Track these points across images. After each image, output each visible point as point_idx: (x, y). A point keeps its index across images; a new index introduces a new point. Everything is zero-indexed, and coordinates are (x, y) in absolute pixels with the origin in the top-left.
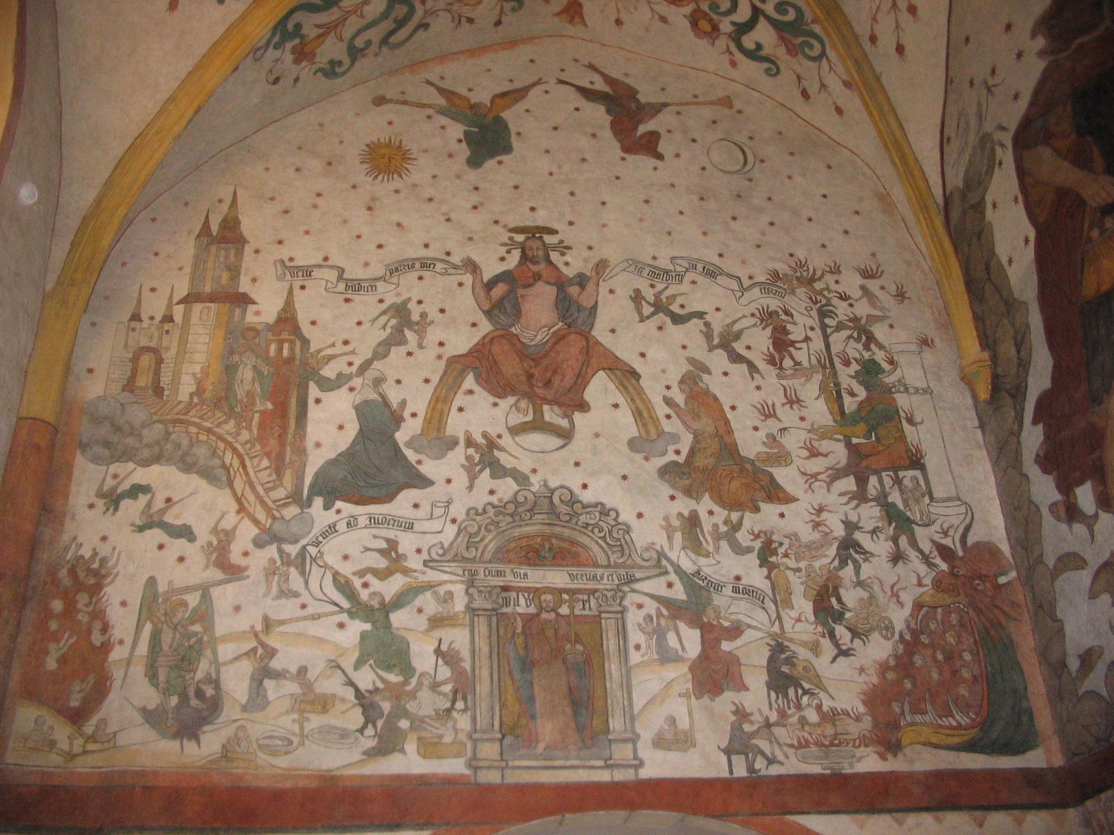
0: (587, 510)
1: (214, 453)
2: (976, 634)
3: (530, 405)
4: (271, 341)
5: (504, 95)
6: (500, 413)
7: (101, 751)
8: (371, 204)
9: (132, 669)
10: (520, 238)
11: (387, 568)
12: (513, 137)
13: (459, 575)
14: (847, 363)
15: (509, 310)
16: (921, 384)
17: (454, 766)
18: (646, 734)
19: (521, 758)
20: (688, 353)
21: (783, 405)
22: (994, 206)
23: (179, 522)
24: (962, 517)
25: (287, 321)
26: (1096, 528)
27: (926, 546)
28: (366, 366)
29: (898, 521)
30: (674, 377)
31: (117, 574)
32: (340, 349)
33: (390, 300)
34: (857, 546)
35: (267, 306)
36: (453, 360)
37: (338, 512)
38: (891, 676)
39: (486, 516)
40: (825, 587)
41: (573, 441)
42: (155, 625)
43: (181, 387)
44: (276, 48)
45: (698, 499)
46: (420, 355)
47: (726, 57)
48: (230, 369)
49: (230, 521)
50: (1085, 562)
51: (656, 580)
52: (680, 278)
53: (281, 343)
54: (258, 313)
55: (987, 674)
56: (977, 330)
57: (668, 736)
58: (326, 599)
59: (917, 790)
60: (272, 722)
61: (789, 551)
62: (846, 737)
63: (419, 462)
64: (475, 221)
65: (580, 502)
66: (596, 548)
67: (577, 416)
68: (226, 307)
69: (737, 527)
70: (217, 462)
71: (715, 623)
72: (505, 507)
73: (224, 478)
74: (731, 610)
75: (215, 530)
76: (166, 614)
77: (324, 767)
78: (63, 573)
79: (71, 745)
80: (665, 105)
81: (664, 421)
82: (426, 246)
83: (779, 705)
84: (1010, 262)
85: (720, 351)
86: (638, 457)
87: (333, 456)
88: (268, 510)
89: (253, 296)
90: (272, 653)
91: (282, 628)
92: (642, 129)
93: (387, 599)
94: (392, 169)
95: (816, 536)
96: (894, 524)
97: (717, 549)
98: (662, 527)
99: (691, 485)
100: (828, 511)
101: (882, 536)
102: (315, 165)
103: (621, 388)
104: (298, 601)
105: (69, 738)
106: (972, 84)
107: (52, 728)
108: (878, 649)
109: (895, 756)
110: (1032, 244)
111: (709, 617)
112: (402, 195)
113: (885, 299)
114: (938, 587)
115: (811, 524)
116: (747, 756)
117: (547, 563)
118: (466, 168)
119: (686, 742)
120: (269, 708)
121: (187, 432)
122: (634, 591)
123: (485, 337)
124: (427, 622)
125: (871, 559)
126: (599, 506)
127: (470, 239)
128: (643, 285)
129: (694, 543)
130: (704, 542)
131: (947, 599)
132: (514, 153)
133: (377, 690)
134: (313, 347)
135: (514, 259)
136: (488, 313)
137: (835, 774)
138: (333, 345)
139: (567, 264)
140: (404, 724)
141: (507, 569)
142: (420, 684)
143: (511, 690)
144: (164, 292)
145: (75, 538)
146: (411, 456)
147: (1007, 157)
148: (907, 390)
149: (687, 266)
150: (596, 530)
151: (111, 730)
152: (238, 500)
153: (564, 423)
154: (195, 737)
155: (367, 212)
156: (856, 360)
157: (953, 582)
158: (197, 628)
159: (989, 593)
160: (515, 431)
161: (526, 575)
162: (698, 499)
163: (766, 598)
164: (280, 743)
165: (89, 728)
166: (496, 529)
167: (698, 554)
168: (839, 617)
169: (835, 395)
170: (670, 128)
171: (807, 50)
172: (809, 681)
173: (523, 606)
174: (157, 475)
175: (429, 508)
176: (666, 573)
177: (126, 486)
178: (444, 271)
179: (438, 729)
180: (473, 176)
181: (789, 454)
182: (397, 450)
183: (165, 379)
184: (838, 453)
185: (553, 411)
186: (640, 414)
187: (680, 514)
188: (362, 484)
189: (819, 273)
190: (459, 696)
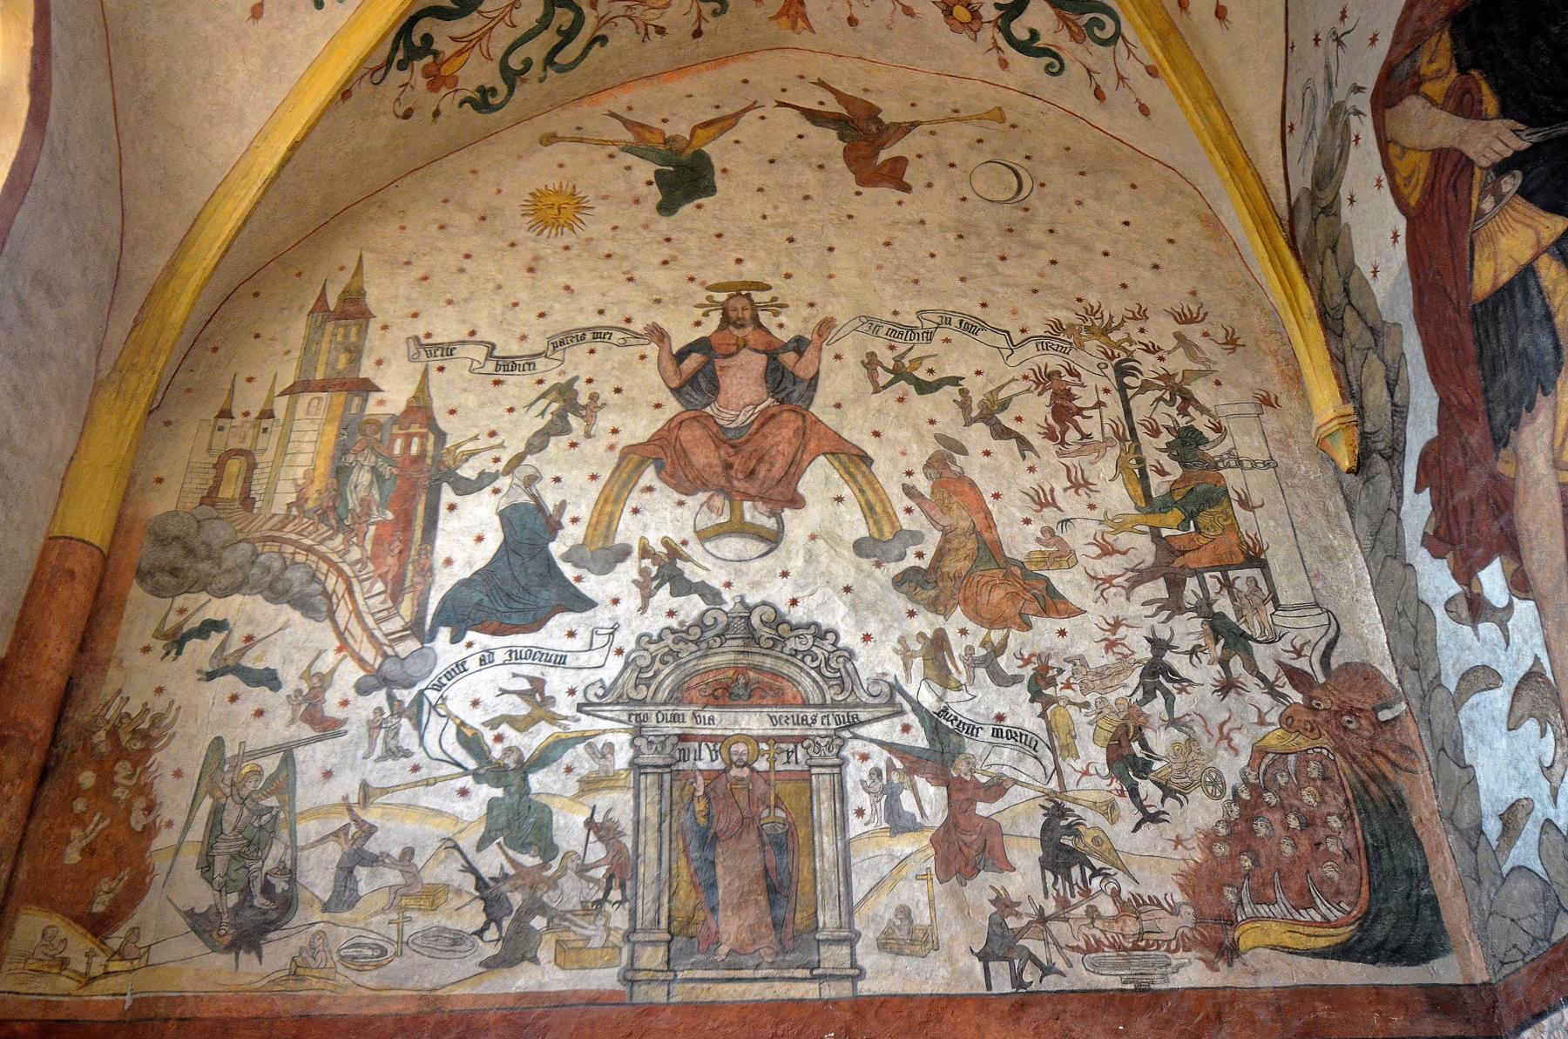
0: (795, 633)
2: (1348, 791)
3: (727, 502)
4: (398, 436)
6: (686, 514)
7: (128, 971)
8: (533, 265)
9: (180, 859)
10: (721, 297)
11: (529, 715)
12: (718, 173)
13: (621, 722)
14: (1155, 433)
15: (703, 386)
17: (605, 979)
18: (869, 935)
19: (694, 967)
20: (935, 429)
21: (1065, 490)
22: (1352, 201)
23: (261, 666)
24: (1323, 630)
25: (420, 410)
26: (1510, 624)
28: (518, 459)
30: (917, 460)
31: (174, 735)
32: (484, 442)
33: (552, 379)
34: (1170, 673)
37: (470, 645)
38: (1221, 850)
39: (662, 644)
41: (781, 545)
42: (216, 800)
43: (277, 496)
44: (402, 66)
45: (946, 616)
46: (586, 446)
47: (994, 54)
48: (340, 472)
50: (1500, 678)
51: (887, 722)
53: (408, 439)
54: (381, 403)
55: (1366, 847)
56: (1337, 377)
57: (901, 934)
58: (445, 758)
60: (362, 925)
61: (1072, 681)
62: (1155, 936)
63: (578, 579)
64: (663, 280)
65: (788, 623)
66: (807, 682)
67: (787, 513)
68: (340, 397)
70: (316, 587)
71: (968, 778)
72: (687, 632)
73: (324, 608)
74: (989, 761)
75: (306, 675)
76: (233, 784)
77: (427, 986)
79: (89, 964)
80: (914, 124)
82: (601, 312)
83: (1058, 894)
84: (1375, 272)
85: (981, 425)
86: (867, 564)
87: (467, 575)
89: (377, 382)
90: (369, 831)
91: (384, 799)
93: (527, 756)
94: (562, 221)
95: (1110, 659)
96: (1222, 642)
97: (972, 678)
98: (896, 651)
99: (937, 597)
100: (1127, 626)
101: (1204, 658)
102: (466, 221)
103: (846, 476)
104: (407, 763)
105: (86, 955)
106: (1317, 40)
107: (64, 941)
109: (1230, 965)
110: (1402, 240)
111: (959, 770)
112: (574, 252)
114: (1290, 726)
115: (1103, 643)
116: (1011, 961)
117: (741, 702)
118: (656, 215)
119: (926, 942)
120: (358, 905)
121: (280, 553)
122: (856, 737)
123: (672, 419)
124: (577, 784)
125: (1189, 689)
126: (813, 627)
127: (658, 301)
128: (879, 346)
129: (940, 672)
130: (953, 670)
131: (1303, 742)
132: (718, 194)
133: (506, 876)
136: (676, 391)
137: (1141, 991)
138: (476, 438)
139: (781, 326)
140: (539, 922)
142: (563, 869)
143: (684, 872)
145: (120, 691)
146: (569, 571)
147: (1364, 127)
148: (1240, 464)
149: (939, 320)
150: (808, 659)
151: (143, 942)
152: (340, 635)
153: (770, 523)
155: (527, 274)
156: (1167, 428)
157: (1310, 719)
158: (272, 801)
159: (1367, 734)
160: (703, 536)
161: (712, 719)
162: (946, 616)
163: (1040, 743)
164: (369, 953)
165: (114, 943)
166: (675, 660)
167: (946, 687)
168: (1143, 769)
170: (920, 152)
171: (1097, 31)
172: (1101, 857)
173: (706, 761)
175: (587, 635)
176: (901, 712)
177: (195, 622)
178: (622, 341)
179: (583, 927)
180: (664, 224)
181: (1072, 552)
183: (258, 487)
184: (1142, 548)
185: (755, 508)
186: (871, 507)
187: (921, 635)
188: (502, 609)
189: (1116, 321)
190: (615, 882)
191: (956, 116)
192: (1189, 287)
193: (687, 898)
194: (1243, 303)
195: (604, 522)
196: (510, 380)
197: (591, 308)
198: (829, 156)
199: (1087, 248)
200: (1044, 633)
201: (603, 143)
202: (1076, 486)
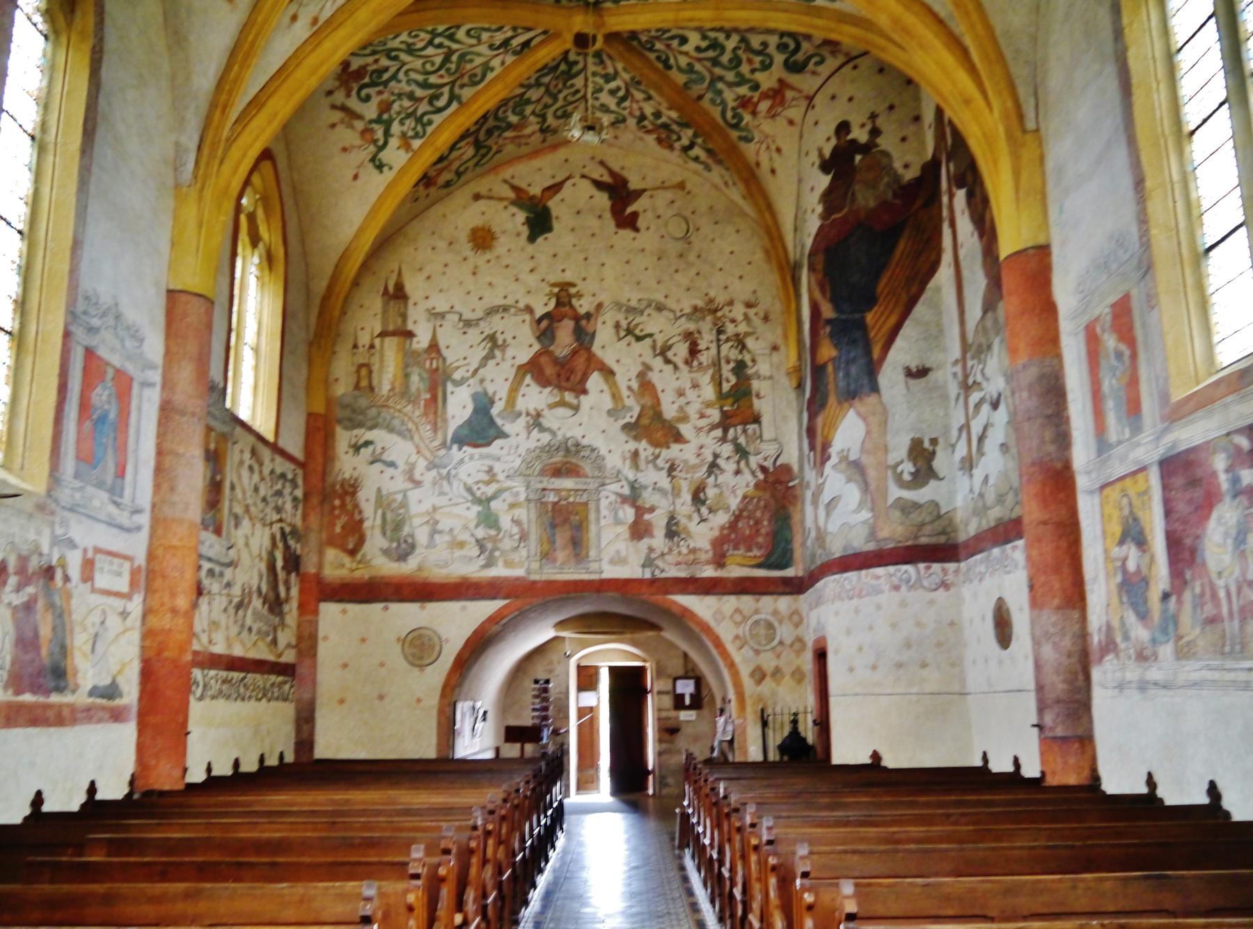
1: (403, 423)
4: (425, 360)
5: (549, 188)
16: (768, 374)
17: (519, 572)
18: (606, 557)
25: (434, 347)
28: (476, 371)
29: (742, 453)
32: (462, 362)
35: (422, 340)
36: (520, 367)
48: (407, 376)
49: (414, 458)
52: (642, 312)
53: (432, 359)
54: (418, 342)
59: (729, 585)
64: (532, 280)
67: (582, 397)
68: (401, 339)
69: (657, 457)
70: (404, 428)
75: (407, 463)
78: (338, 487)
80: (644, 191)
86: (612, 420)
88: (431, 452)
90: (437, 522)
92: (629, 210)
97: (647, 468)
102: (442, 245)
108: (722, 518)
111: (639, 503)
113: (757, 321)
128: (621, 317)
131: (760, 494)
134: (448, 362)
136: (538, 338)
141: (545, 479)
142: (504, 536)
144: (368, 331)
146: (499, 421)
151: (368, 558)
152: (417, 447)
153: (575, 402)
160: (552, 406)
165: (359, 557)
168: (703, 502)
169: (718, 381)
173: (552, 498)
176: (620, 481)
177: (361, 441)
180: (530, 248)
184: (715, 415)
191: (663, 187)
192: (752, 289)
193: (546, 547)
195: (511, 401)
197: (502, 295)
200: (674, 451)
201: (501, 199)
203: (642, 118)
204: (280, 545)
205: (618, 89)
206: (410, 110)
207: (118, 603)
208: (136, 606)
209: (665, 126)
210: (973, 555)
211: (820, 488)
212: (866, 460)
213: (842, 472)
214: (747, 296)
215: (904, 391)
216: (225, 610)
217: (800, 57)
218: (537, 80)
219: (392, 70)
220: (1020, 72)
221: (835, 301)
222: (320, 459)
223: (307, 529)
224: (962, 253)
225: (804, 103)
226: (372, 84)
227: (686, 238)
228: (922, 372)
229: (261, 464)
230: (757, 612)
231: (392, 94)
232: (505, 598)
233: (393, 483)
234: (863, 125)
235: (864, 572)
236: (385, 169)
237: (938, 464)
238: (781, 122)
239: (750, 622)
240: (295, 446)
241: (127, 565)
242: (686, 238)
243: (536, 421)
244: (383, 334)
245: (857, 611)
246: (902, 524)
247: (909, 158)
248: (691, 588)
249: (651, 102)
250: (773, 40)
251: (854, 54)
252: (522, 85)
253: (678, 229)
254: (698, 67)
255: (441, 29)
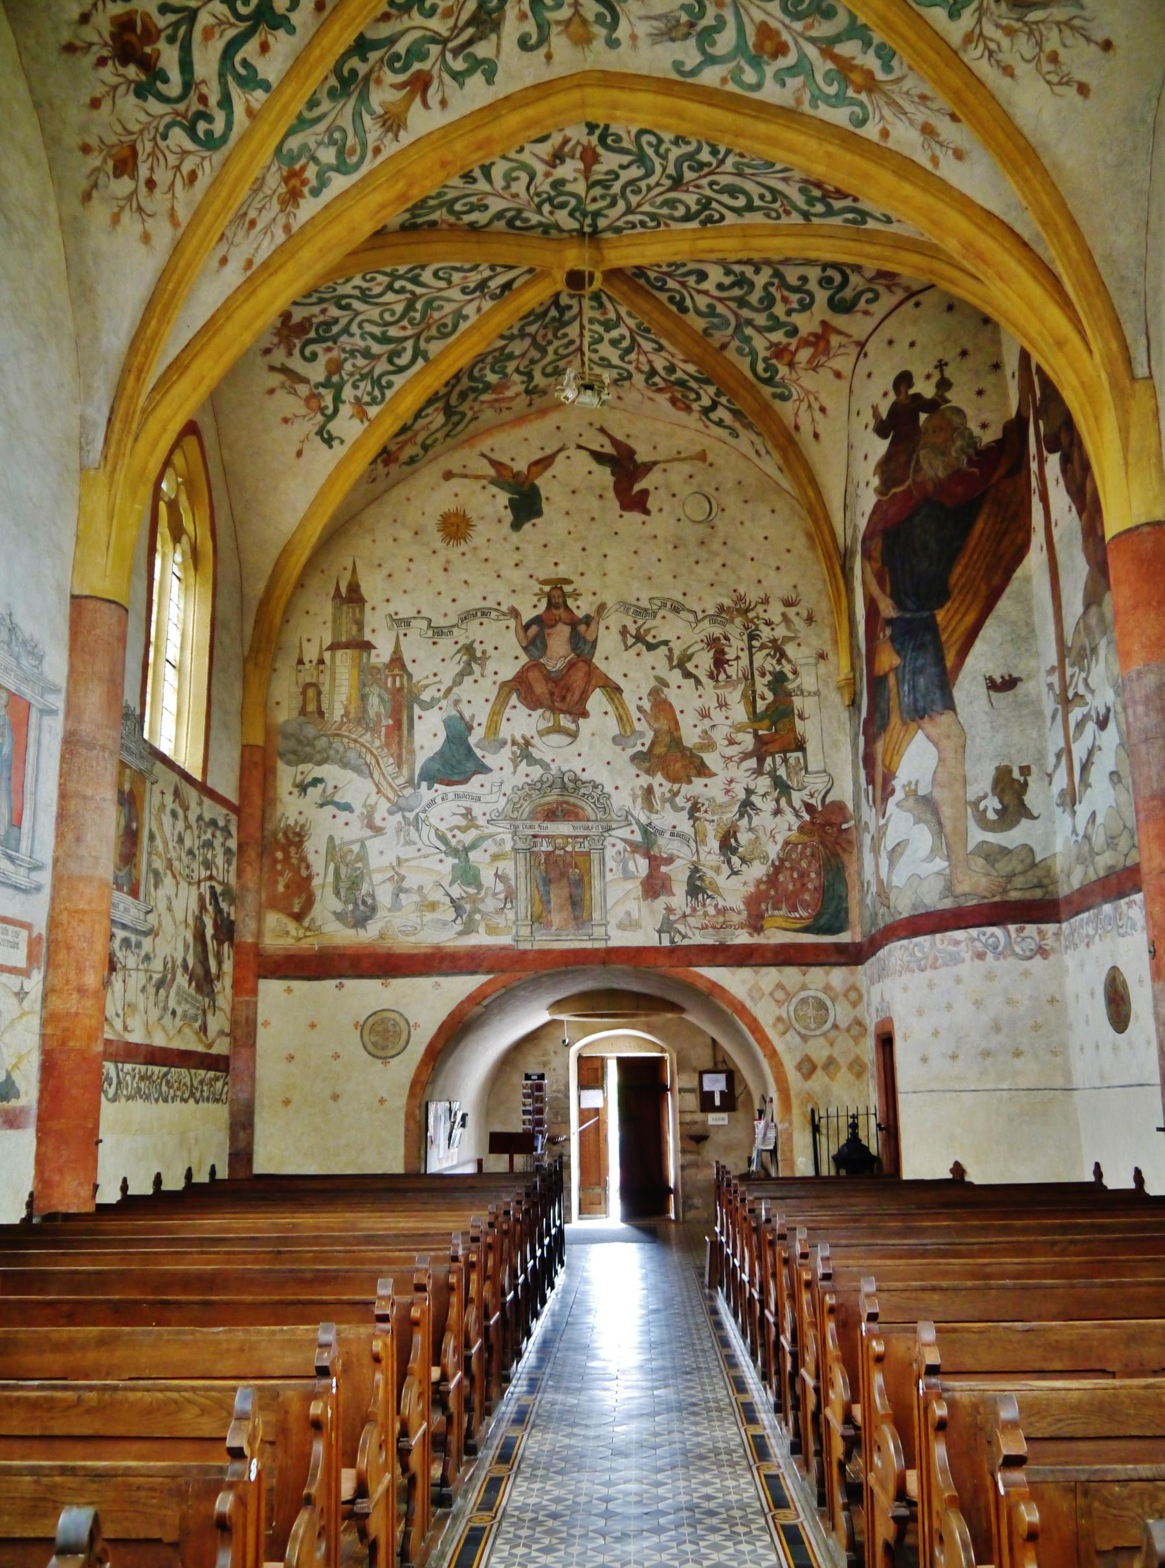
5: (537, 463)
6: (532, 720)
10: (547, 588)
14: (763, 675)
16: (813, 689)
17: (505, 940)
20: (656, 672)
23: (343, 801)
25: (397, 661)
27: (797, 804)
28: (449, 690)
29: (782, 787)
30: (645, 692)
32: (432, 679)
33: (463, 641)
34: (752, 805)
35: (383, 653)
36: (504, 684)
40: (728, 832)
46: (481, 680)
48: (364, 698)
52: (654, 615)
53: (394, 677)
59: (769, 954)
64: (517, 577)
67: (581, 721)
68: (356, 652)
69: (676, 794)
75: (365, 805)
81: (636, 723)
86: (618, 749)
89: (374, 642)
90: (403, 878)
95: (727, 798)
102: (406, 535)
104: (415, 847)
108: (758, 870)
111: (655, 851)
113: (798, 623)
128: (628, 621)
129: (649, 804)
131: (806, 839)
135: (543, 605)
136: (525, 649)
140: (478, 917)
141: (536, 824)
146: (479, 753)
151: (318, 923)
153: (573, 727)
154: (364, 927)
158: (359, 865)
160: (542, 733)
162: (653, 776)
165: (306, 923)
168: (734, 851)
169: (751, 699)
173: (545, 847)
174: (327, 771)
177: (309, 779)
180: (515, 537)
182: (469, 749)
191: (679, 458)
192: (792, 583)
193: (538, 908)
194: (820, 593)
195: (493, 726)
196: (440, 641)
197: (480, 597)
198: (605, 488)
199: (743, 556)
200: (697, 787)
201: (478, 477)
202: (721, 706)
203: (653, 372)
204: (210, 908)
205: (623, 337)
206: (365, 371)
207: (13, 981)
208: (35, 984)
209: (681, 383)
210: (1077, 914)
211: (882, 832)
212: (938, 795)
213: (909, 811)
214: (786, 592)
215: (987, 708)
216: (144, 989)
217: (848, 293)
218: (522, 329)
219: (343, 322)
220: (1127, 307)
221: (897, 598)
222: (257, 801)
223: (243, 888)
224: (1056, 533)
225: (854, 350)
226: (320, 340)
227: (708, 522)
228: (1009, 684)
229: (186, 809)
230: (804, 987)
231: (344, 351)
232: (488, 972)
233: (348, 830)
234: (928, 377)
235: (938, 936)
236: (336, 443)
237: (1031, 799)
238: (826, 375)
239: (795, 1001)
240: (226, 784)
241: (24, 934)
242: (708, 522)
243: (524, 751)
244: (334, 647)
245: (931, 986)
246: (987, 875)
247: (986, 416)
248: (720, 958)
249: (663, 354)
250: (814, 274)
251: (915, 288)
252: (502, 337)
253: (698, 510)
254: (720, 308)
255: (402, 270)
